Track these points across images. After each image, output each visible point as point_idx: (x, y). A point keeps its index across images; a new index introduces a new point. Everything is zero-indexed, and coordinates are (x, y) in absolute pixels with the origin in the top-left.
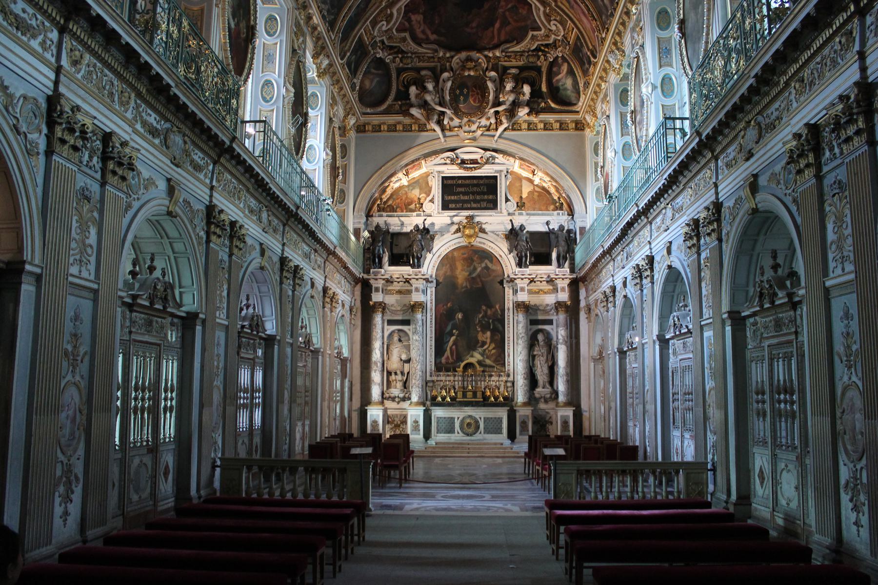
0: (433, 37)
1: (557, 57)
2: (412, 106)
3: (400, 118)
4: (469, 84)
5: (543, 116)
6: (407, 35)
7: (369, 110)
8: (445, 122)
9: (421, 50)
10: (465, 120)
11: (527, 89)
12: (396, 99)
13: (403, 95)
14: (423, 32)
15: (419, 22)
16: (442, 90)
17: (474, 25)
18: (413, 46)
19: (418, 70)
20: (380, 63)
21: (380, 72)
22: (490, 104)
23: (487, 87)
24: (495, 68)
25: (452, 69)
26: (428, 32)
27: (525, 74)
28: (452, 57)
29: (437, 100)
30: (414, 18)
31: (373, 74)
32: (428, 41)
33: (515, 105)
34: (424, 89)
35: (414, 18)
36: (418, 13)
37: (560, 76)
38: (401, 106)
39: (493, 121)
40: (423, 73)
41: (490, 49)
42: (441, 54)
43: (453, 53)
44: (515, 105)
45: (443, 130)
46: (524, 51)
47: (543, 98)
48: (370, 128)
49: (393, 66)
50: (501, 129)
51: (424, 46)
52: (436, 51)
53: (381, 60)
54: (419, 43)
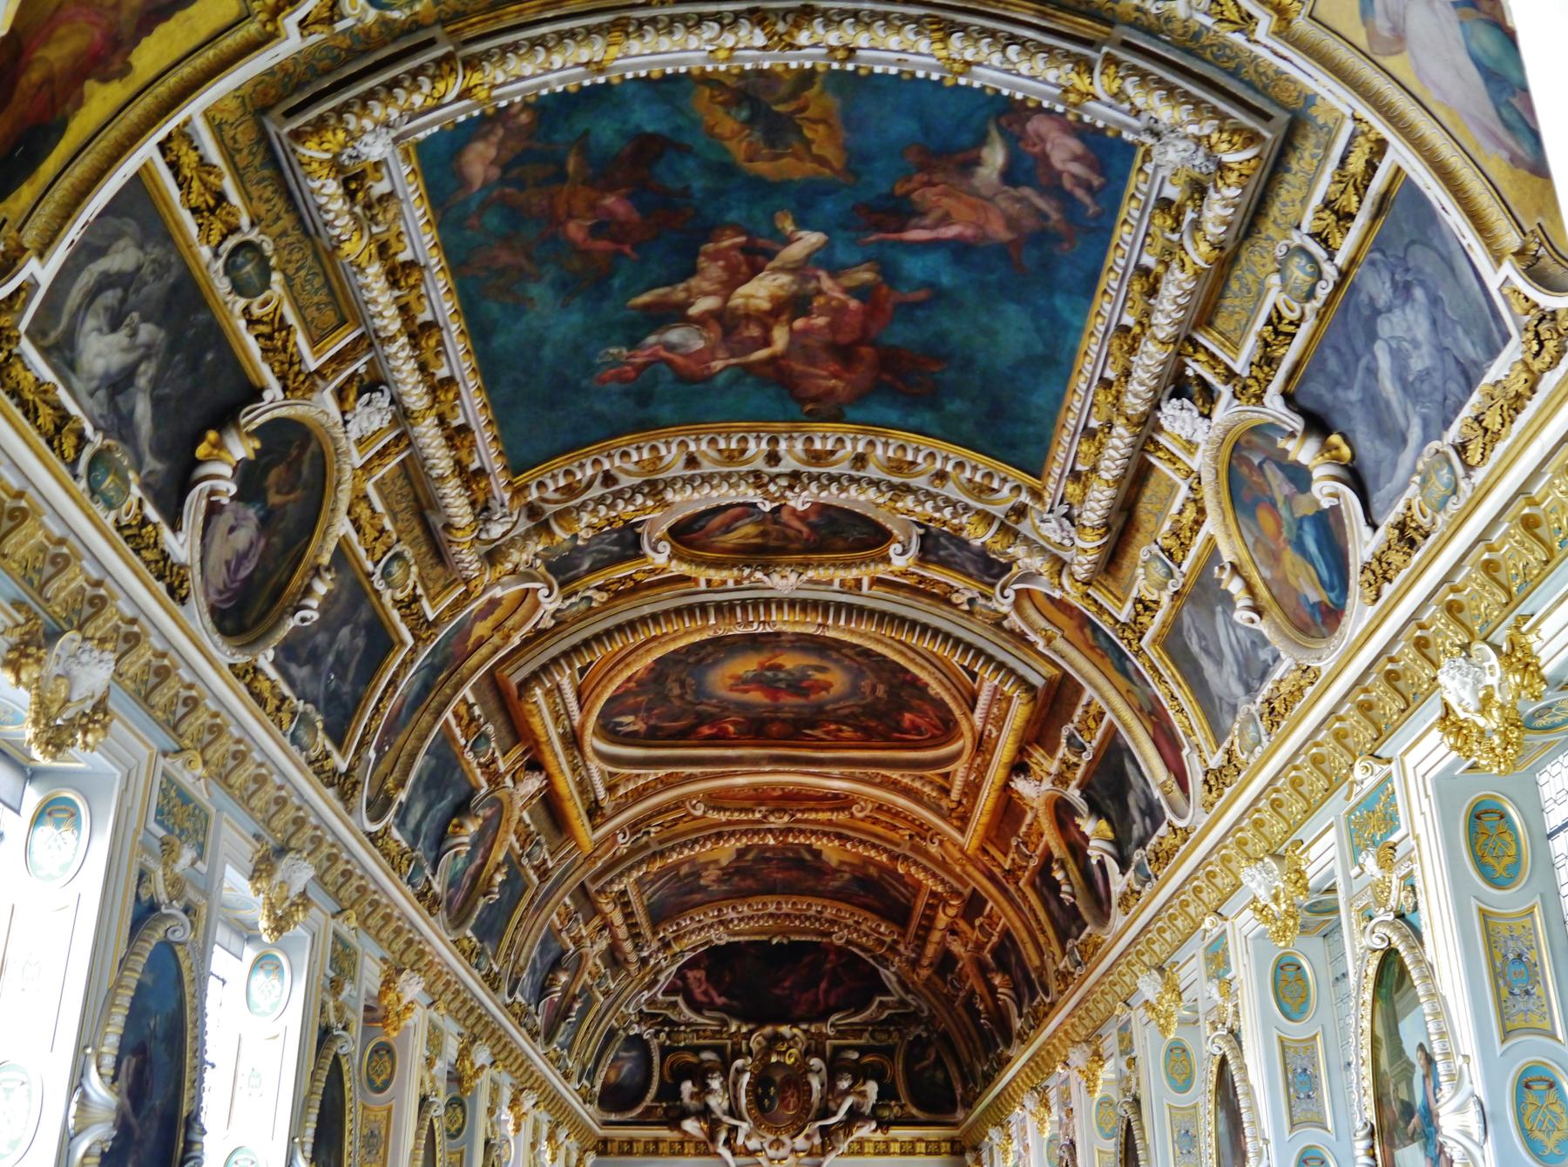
0: (720, 1000)
1: (919, 1037)
2: (685, 1114)
3: (664, 1133)
4: (778, 1079)
5: (895, 1132)
6: (680, 999)
7: (613, 1117)
8: (740, 1141)
9: (700, 1020)
10: (771, 1137)
11: (872, 1088)
12: (657, 1098)
13: (670, 1092)
14: (705, 993)
15: (699, 980)
16: (735, 1084)
17: (787, 984)
18: (689, 1014)
19: (697, 1050)
20: (636, 1042)
21: (633, 1054)
22: (813, 1110)
23: (809, 1084)
24: (820, 1054)
25: (750, 1052)
26: (714, 994)
27: (867, 1059)
28: (751, 1032)
29: (725, 1105)
30: (690, 974)
31: (623, 1059)
32: (712, 1006)
33: (855, 1116)
34: (704, 1089)
35: (690, 974)
36: (699, 968)
37: (926, 1063)
38: (666, 1110)
39: (817, 1140)
40: (706, 1056)
41: (810, 1021)
42: (733, 1029)
43: (751, 1026)
44: (855, 1116)
45: (734, 1154)
46: (865, 1023)
47: (897, 1098)
48: (616, 1150)
49: (654, 1043)
50: (831, 1157)
51: (707, 1014)
52: (725, 1024)
53: (639, 1036)
54: (696, 1007)
